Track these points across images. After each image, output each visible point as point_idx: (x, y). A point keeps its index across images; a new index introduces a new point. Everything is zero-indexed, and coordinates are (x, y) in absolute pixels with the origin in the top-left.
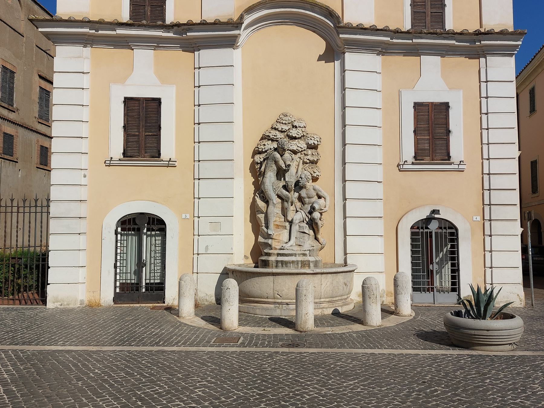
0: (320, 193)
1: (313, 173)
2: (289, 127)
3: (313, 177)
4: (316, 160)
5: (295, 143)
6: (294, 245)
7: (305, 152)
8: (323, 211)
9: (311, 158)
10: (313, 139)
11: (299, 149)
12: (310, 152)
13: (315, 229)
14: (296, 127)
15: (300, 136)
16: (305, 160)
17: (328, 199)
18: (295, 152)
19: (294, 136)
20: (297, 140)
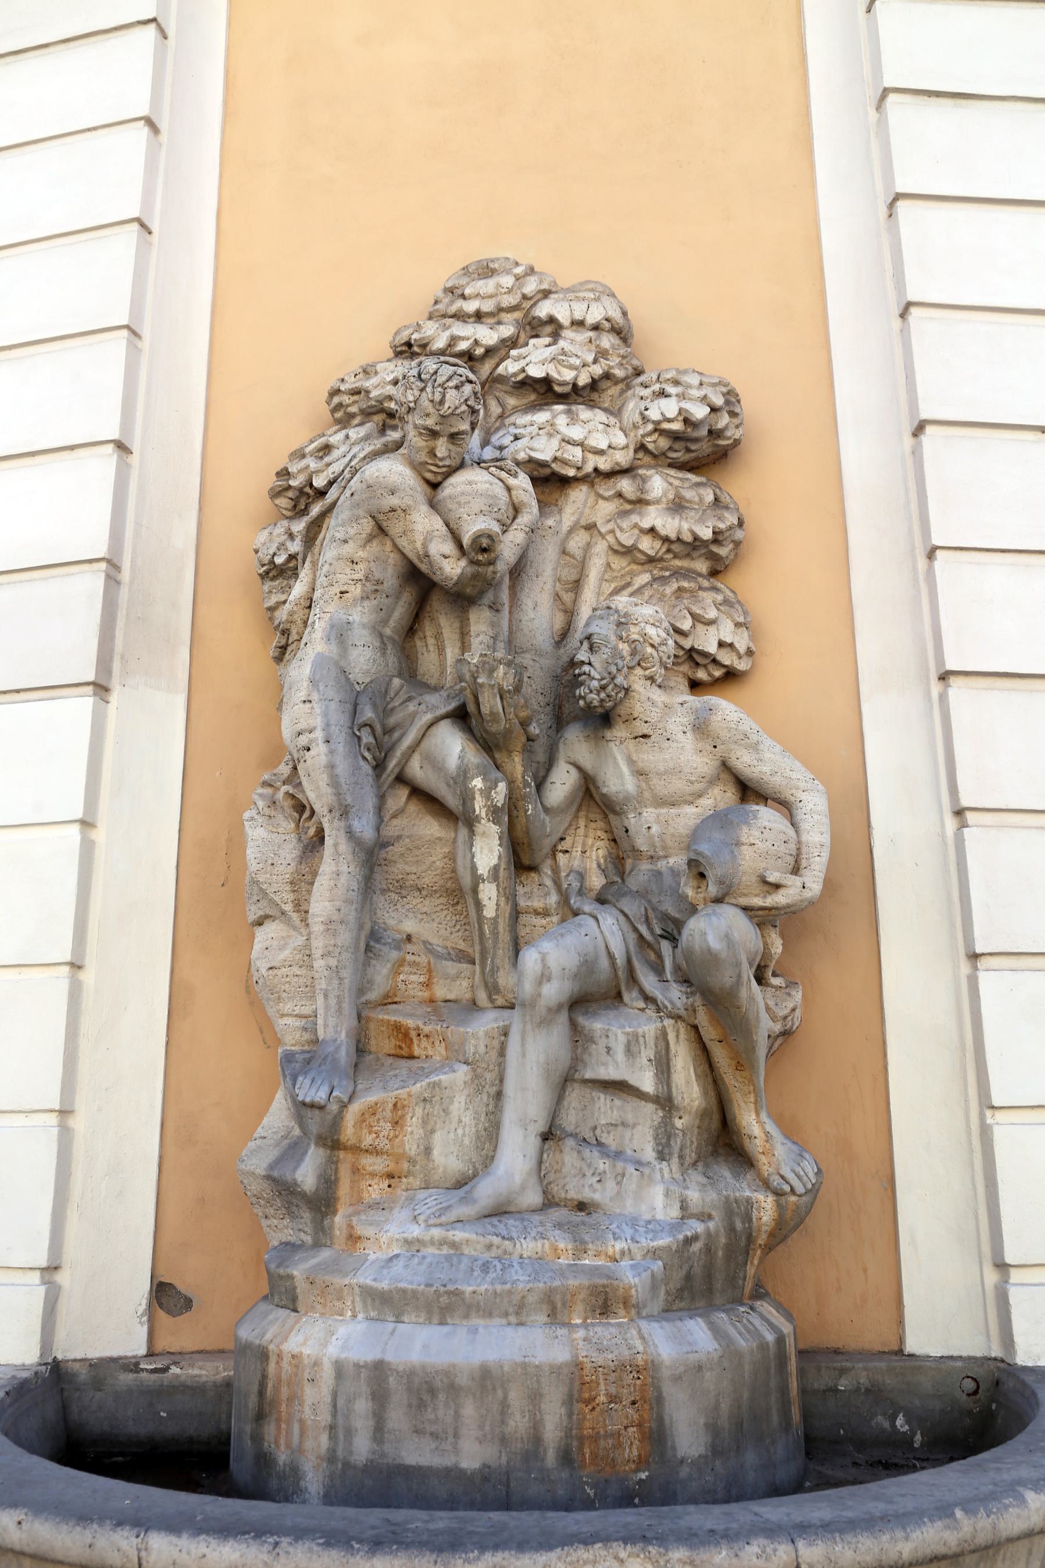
0: (744, 761)
1: (686, 625)
2: (507, 331)
3: (693, 656)
4: (706, 534)
5: (542, 417)
6: (533, 1197)
7: (625, 485)
8: (780, 899)
9: (669, 525)
10: (671, 389)
11: (575, 454)
12: (658, 484)
13: (720, 1055)
14: (553, 327)
15: (583, 380)
16: (627, 540)
17: (814, 805)
18: (550, 481)
19: (536, 372)
20: (559, 408)
